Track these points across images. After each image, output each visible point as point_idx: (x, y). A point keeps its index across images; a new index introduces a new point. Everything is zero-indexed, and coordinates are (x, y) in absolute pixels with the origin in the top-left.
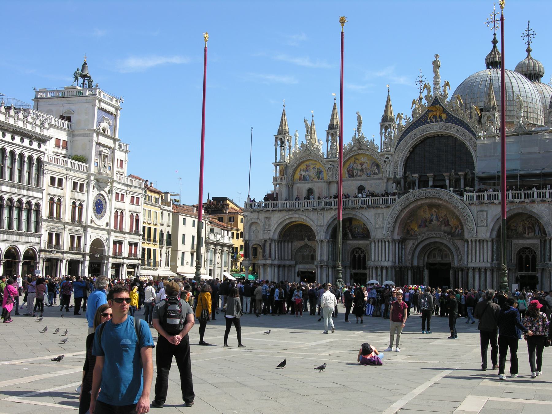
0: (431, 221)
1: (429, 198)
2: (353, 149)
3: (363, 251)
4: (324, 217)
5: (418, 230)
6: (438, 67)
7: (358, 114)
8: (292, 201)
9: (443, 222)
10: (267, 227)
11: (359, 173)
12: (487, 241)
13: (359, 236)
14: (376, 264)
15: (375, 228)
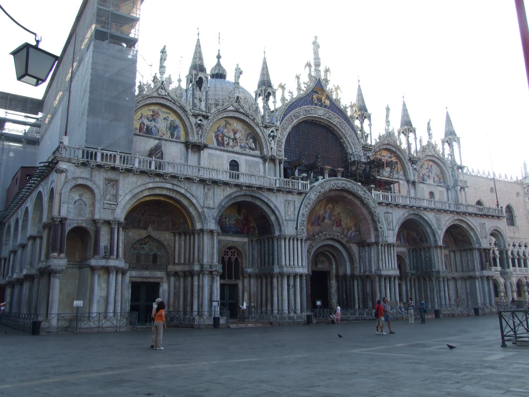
0: (324, 219)
1: (343, 190)
2: (229, 109)
3: (234, 252)
4: (214, 194)
5: (311, 229)
6: (318, 47)
7: (238, 65)
8: (161, 160)
9: (335, 221)
10: (108, 197)
11: (231, 143)
12: (394, 246)
13: (231, 230)
14: (290, 270)
15: (286, 220)
